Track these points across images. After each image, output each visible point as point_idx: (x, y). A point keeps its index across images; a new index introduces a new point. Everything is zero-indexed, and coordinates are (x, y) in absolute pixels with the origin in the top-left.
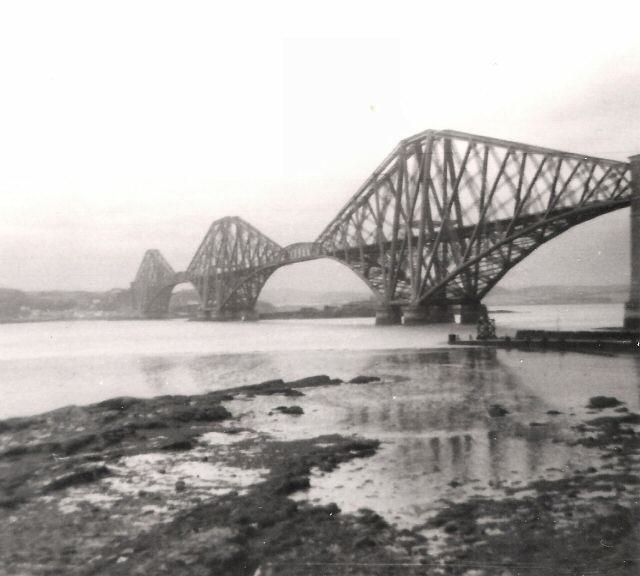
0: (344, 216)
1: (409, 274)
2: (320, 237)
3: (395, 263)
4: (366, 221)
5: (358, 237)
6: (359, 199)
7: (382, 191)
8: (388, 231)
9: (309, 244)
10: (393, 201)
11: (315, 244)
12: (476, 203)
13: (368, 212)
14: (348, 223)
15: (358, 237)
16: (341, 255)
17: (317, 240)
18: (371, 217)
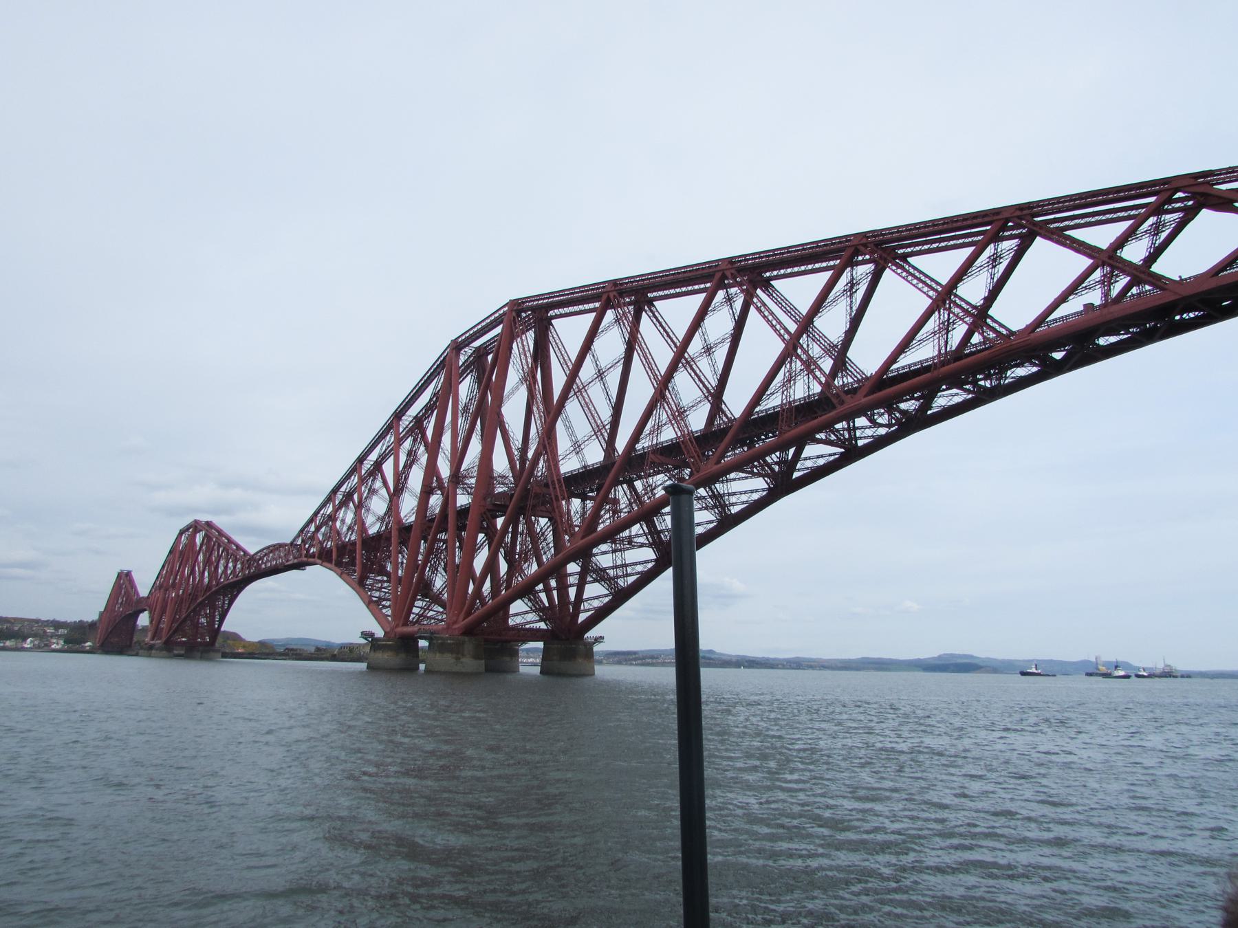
0: (339, 496)
1: (439, 582)
2: (302, 531)
3: (413, 566)
4: (374, 497)
5: (360, 522)
6: (367, 465)
7: (407, 444)
8: (408, 507)
9: (286, 545)
10: (424, 459)
11: (292, 544)
12: (597, 431)
13: (378, 484)
14: (347, 507)
15: (360, 522)
16: (325, 557)
17: (294, 540)
18: (384, 492)
